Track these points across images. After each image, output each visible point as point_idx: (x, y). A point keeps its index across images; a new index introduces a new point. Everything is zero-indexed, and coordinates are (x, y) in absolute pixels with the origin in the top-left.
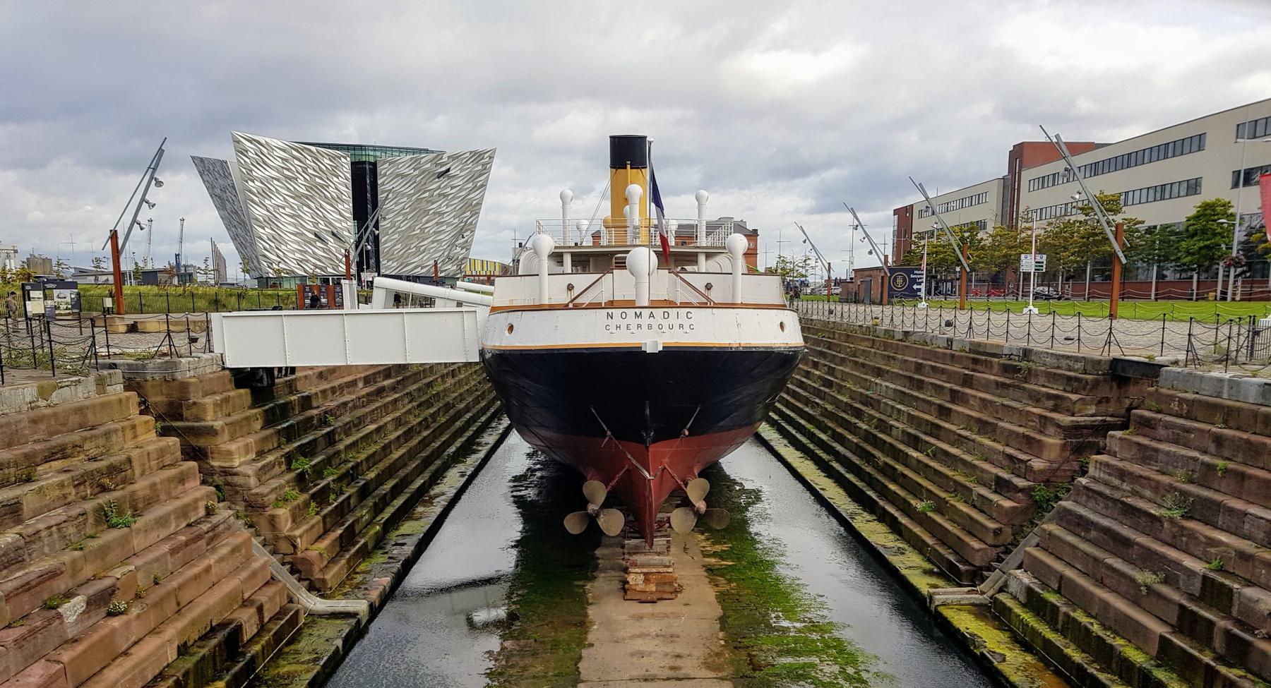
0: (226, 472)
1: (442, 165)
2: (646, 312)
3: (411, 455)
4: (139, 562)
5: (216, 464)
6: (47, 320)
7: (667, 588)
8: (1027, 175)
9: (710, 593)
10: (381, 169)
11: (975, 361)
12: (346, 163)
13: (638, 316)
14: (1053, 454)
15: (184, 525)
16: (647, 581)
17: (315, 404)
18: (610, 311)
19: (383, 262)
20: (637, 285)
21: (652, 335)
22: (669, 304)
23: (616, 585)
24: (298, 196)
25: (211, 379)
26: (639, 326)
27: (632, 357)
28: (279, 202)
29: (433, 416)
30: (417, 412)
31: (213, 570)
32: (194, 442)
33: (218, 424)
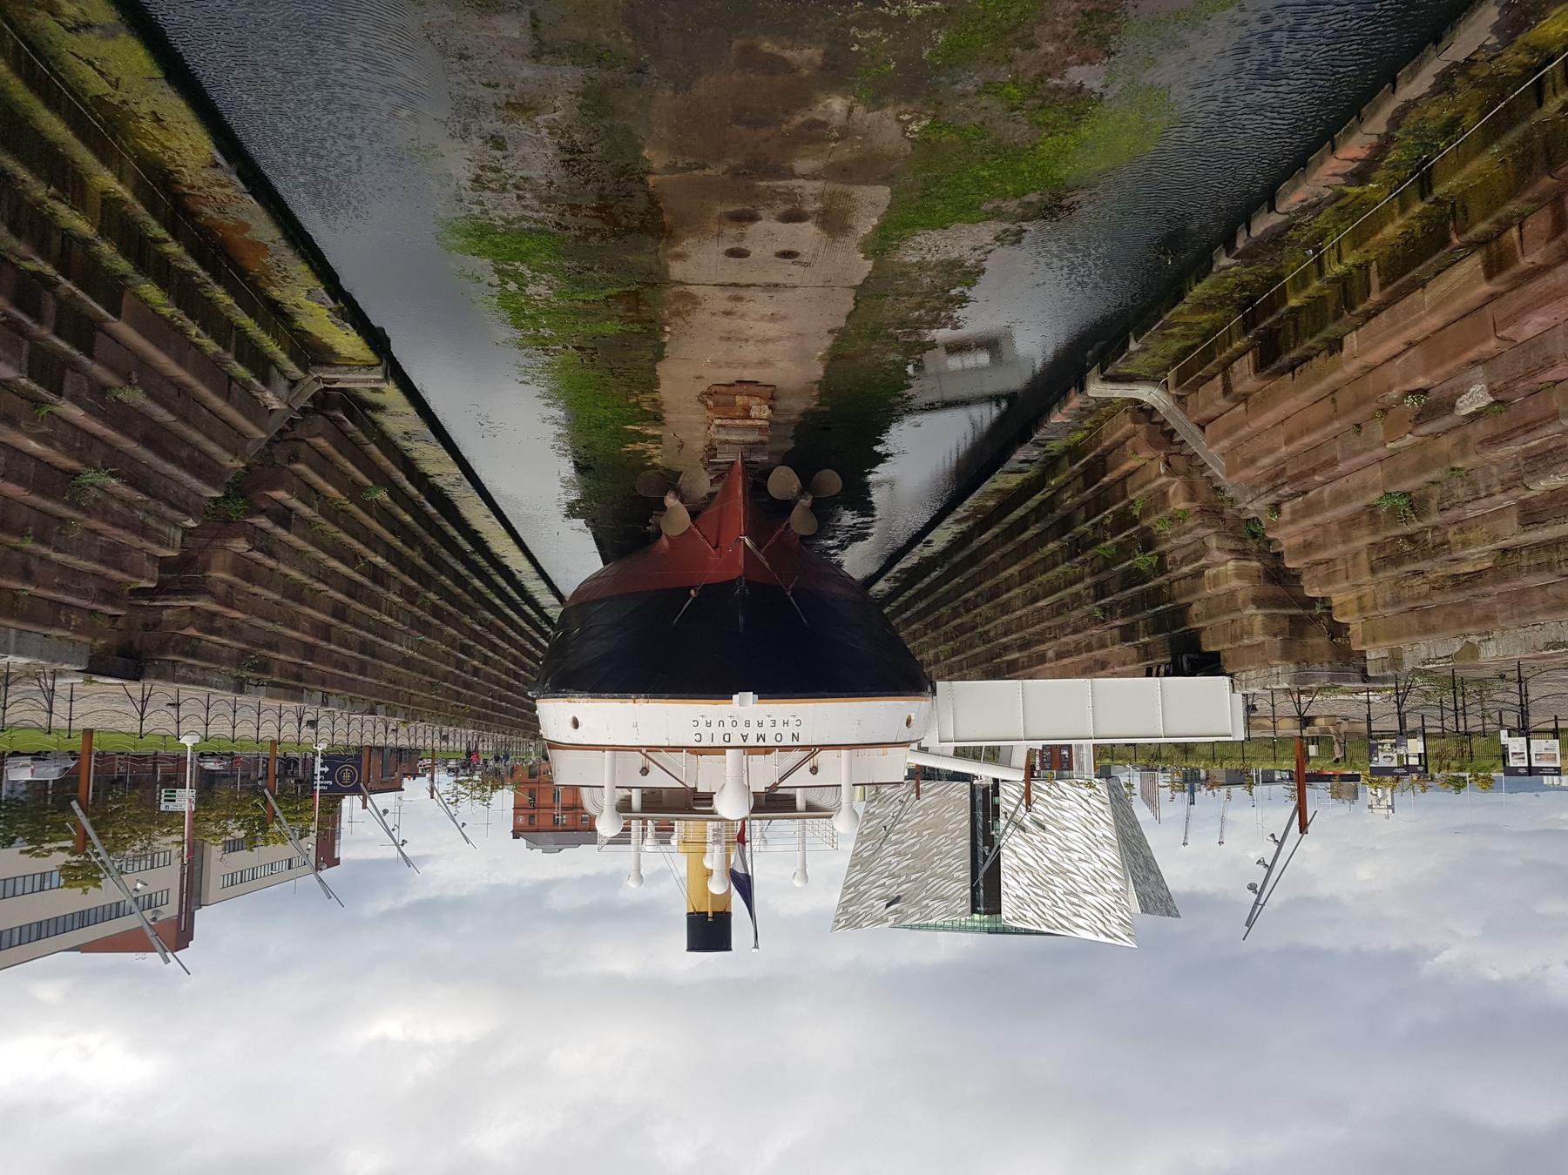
0: (1242, 554)
1: (895, 912)
3: (995, 569)
4: (1380, 452)
5: (1255, 564)
6: (1403, 734)
7: (722, 399)
8: (171, 910)
9: (665, 391)
11: (299, 678)
12: (1006, 912)
14: (219, 558)
15: (1311, 494)
16: (747, 409)
17: (1116, 632)
21: (746, 713)
23: (781, 405)
26: (760, 724)
27: (769, 689)
28: (1085, 865)
29: (956, 614)
30: (978, 620)
31: (1282, 438)
32: (1278, 590)
33: (1251, 610)
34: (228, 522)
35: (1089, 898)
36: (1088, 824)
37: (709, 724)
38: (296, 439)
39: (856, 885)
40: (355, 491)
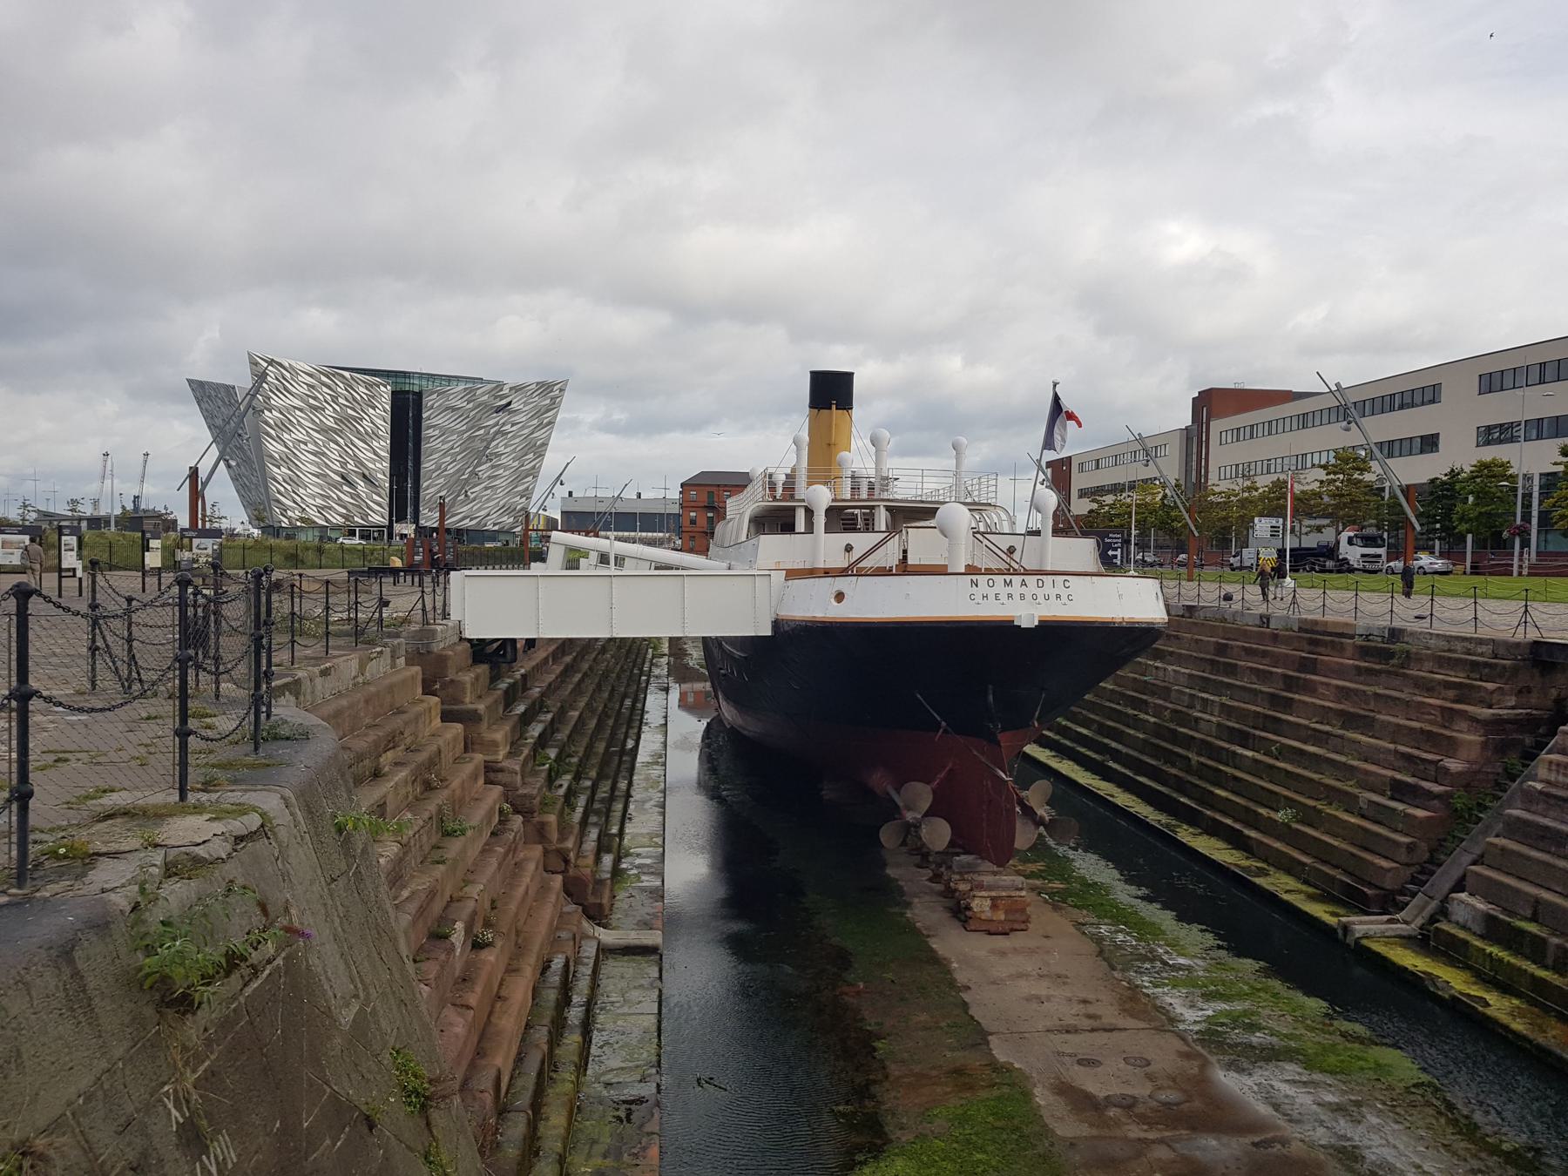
7: (1018, 916)
8: (1217, 426)
10: (428, 401)
11: (1312, 642)
12: (385, 392)
13: (1008, 584)
14: (1474, 753)
16: (994, 907)
20: (952, 549)
24: (324, 430)
26: (1010, 596)
27: (1003, 631)
28: (301, 437)
34: (1467, 786)
35: (297, 403)
36: (295, 481)
37: (1058, 596)
38: (1407, 865)
39: (540, 426)
40: (1311, 817)
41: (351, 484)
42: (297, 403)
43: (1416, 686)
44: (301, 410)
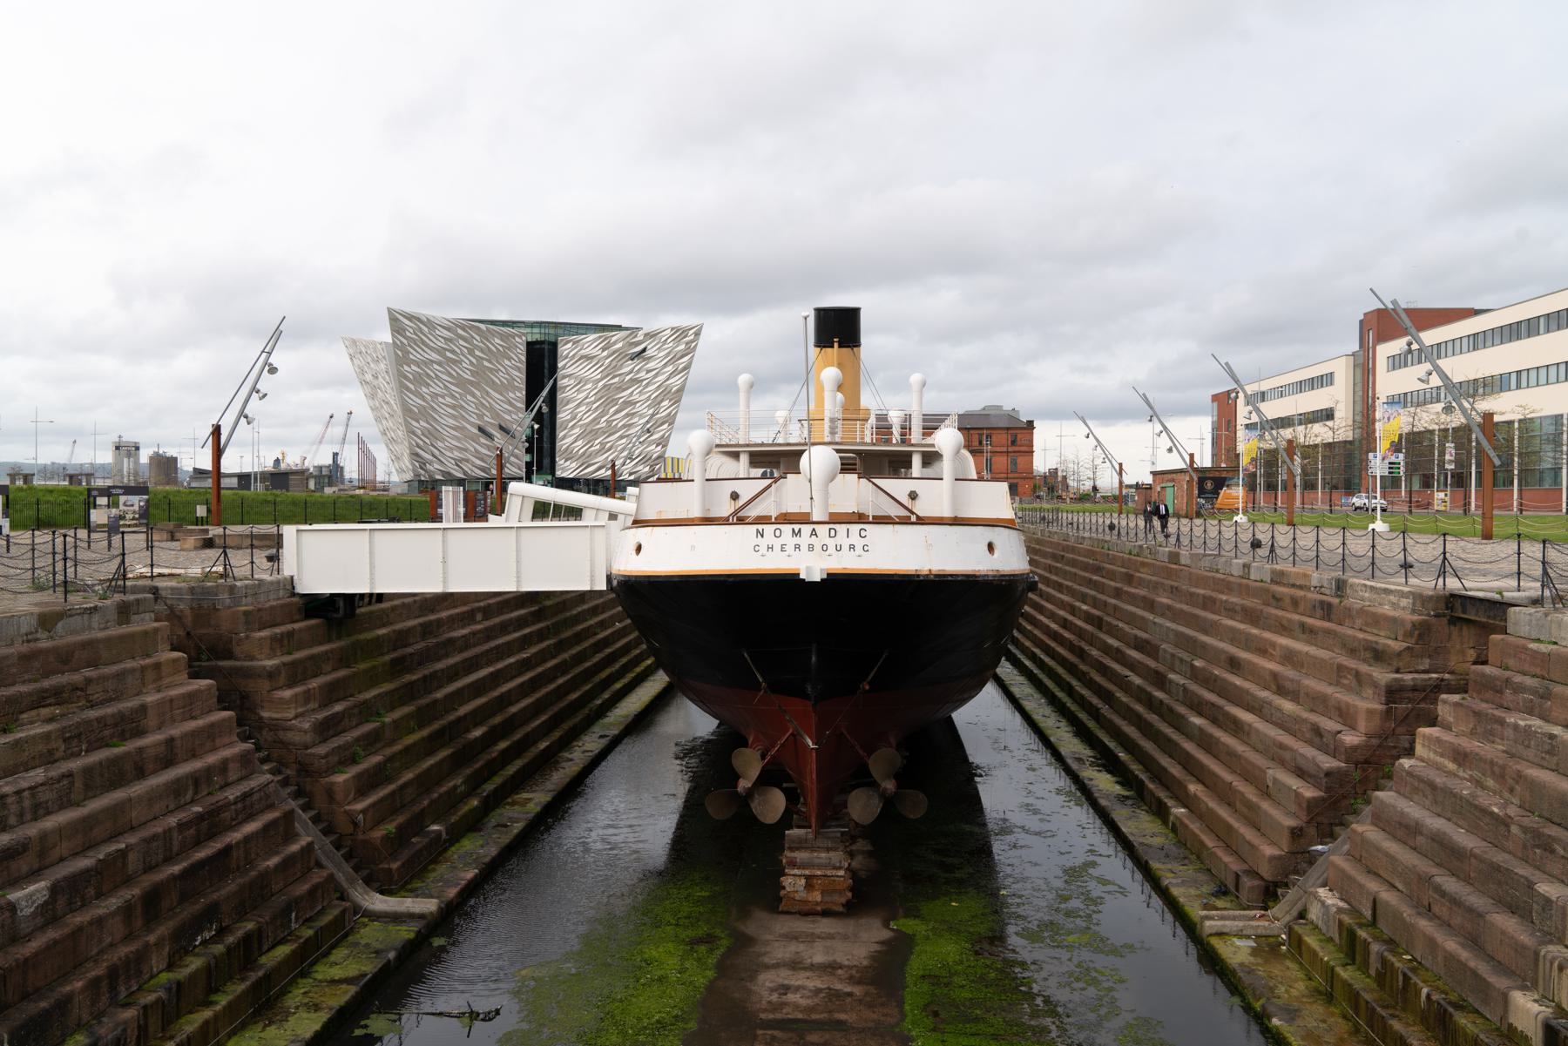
0: (275, 726)
2: (823, 530)
3: (537, 708)
4: (132, 839)
5: (266, 714)
6: (113, 528)
10: (565, 349)
16: (809, 886)
18: (760, 527)
19: (560, 462)
21: (811, 558)
22: (859, 518)
24: (460, 382)
25: (273, 608)
26: (797, 547)
27: (785, 586)
28: (438, 390)
35: (435, 356)
41: (490, 436)
42: (435, 356)
43: (1344, 645)
44: (439, 364)
